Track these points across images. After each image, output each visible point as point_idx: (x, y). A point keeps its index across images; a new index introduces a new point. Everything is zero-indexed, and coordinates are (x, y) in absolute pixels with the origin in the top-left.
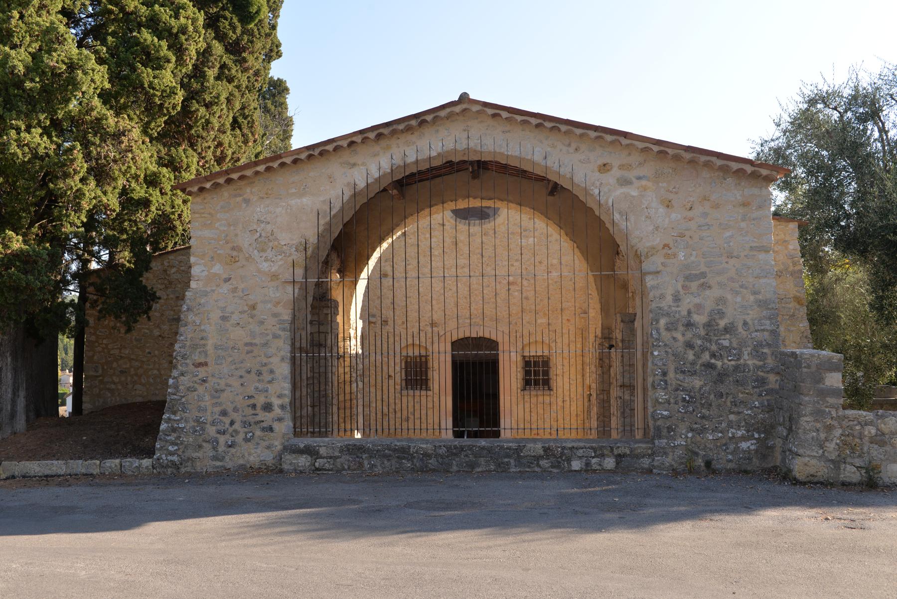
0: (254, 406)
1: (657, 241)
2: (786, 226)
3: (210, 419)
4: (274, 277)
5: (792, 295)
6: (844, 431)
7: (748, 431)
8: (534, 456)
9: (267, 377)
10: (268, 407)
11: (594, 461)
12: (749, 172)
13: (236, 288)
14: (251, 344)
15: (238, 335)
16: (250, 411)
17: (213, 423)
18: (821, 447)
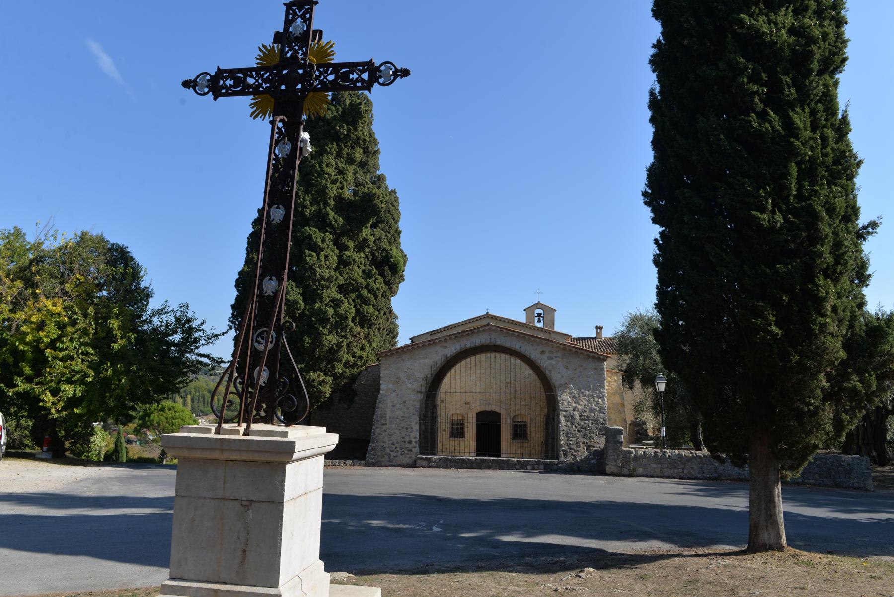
1: (562, 382)
4: (414, 390)
9: (410, 430)
10: (410, 442)
15: (399, 413)
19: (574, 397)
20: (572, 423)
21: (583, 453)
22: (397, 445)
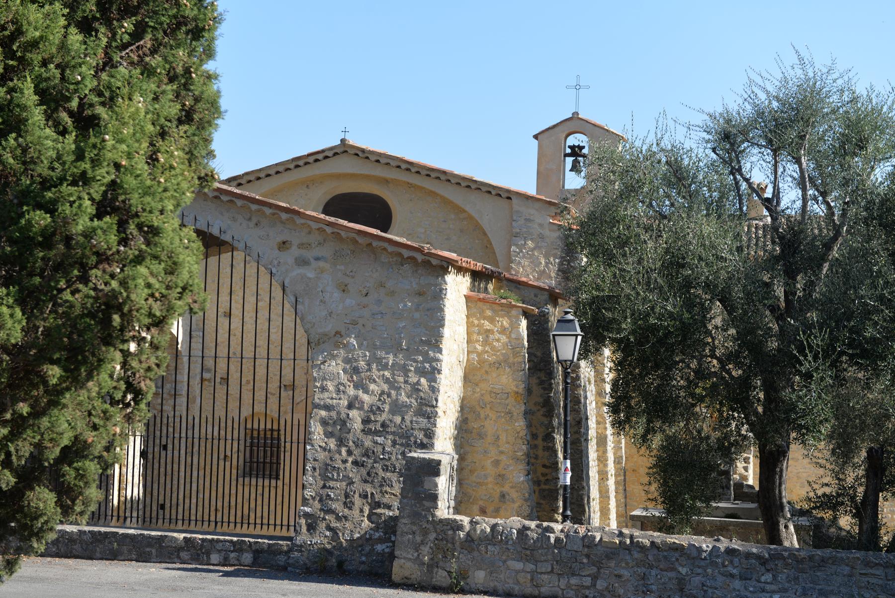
1: (329, 327)
6: (438, 534)
7: (385, 533)
8: (175, 547)
11: (232, 555)
12: (420, 260)
18: (417, 550)
19: (356, 370)
20: (341, 442)
21: (358, 524)
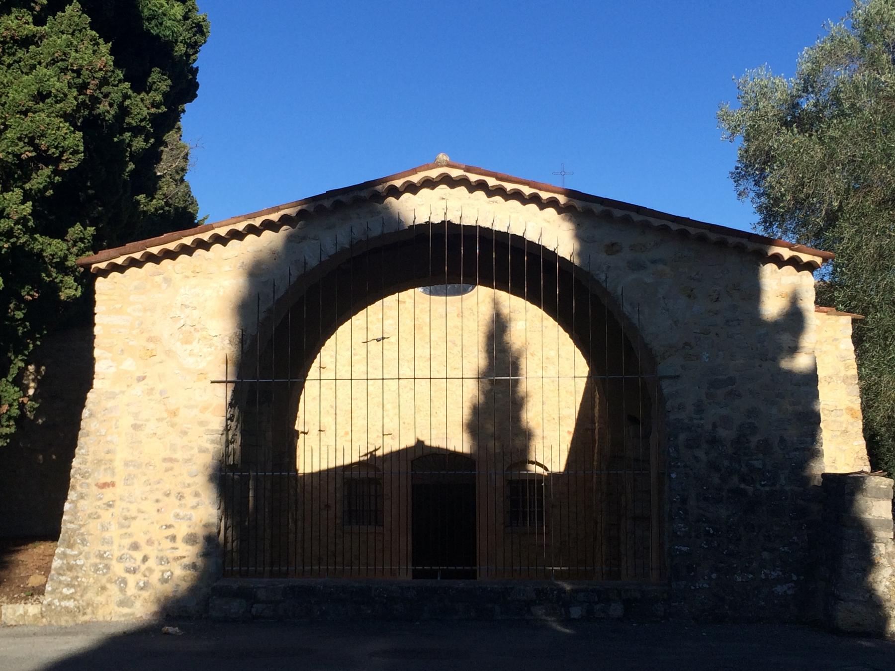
0: (173, 538)
2: (837, 321)
3: (117, 554)
4: (202, 374)
5: (843, 407)
11: (598, 607)
13: (152, 389)
14: (171, 460)
16: (168, 544)
17: (121, 559)
22: (146, 550)
